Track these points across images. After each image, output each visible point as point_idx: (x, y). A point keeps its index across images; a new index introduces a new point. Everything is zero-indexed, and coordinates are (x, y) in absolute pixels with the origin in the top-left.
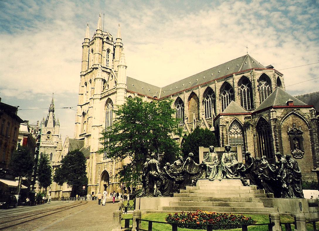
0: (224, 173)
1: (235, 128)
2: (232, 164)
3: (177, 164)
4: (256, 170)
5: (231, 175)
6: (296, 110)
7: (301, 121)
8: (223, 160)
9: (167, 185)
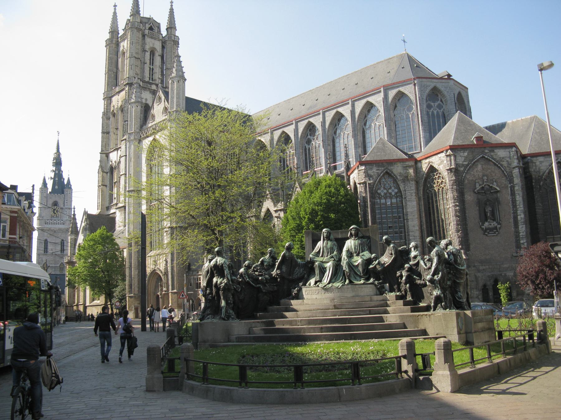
7: (497, 171)
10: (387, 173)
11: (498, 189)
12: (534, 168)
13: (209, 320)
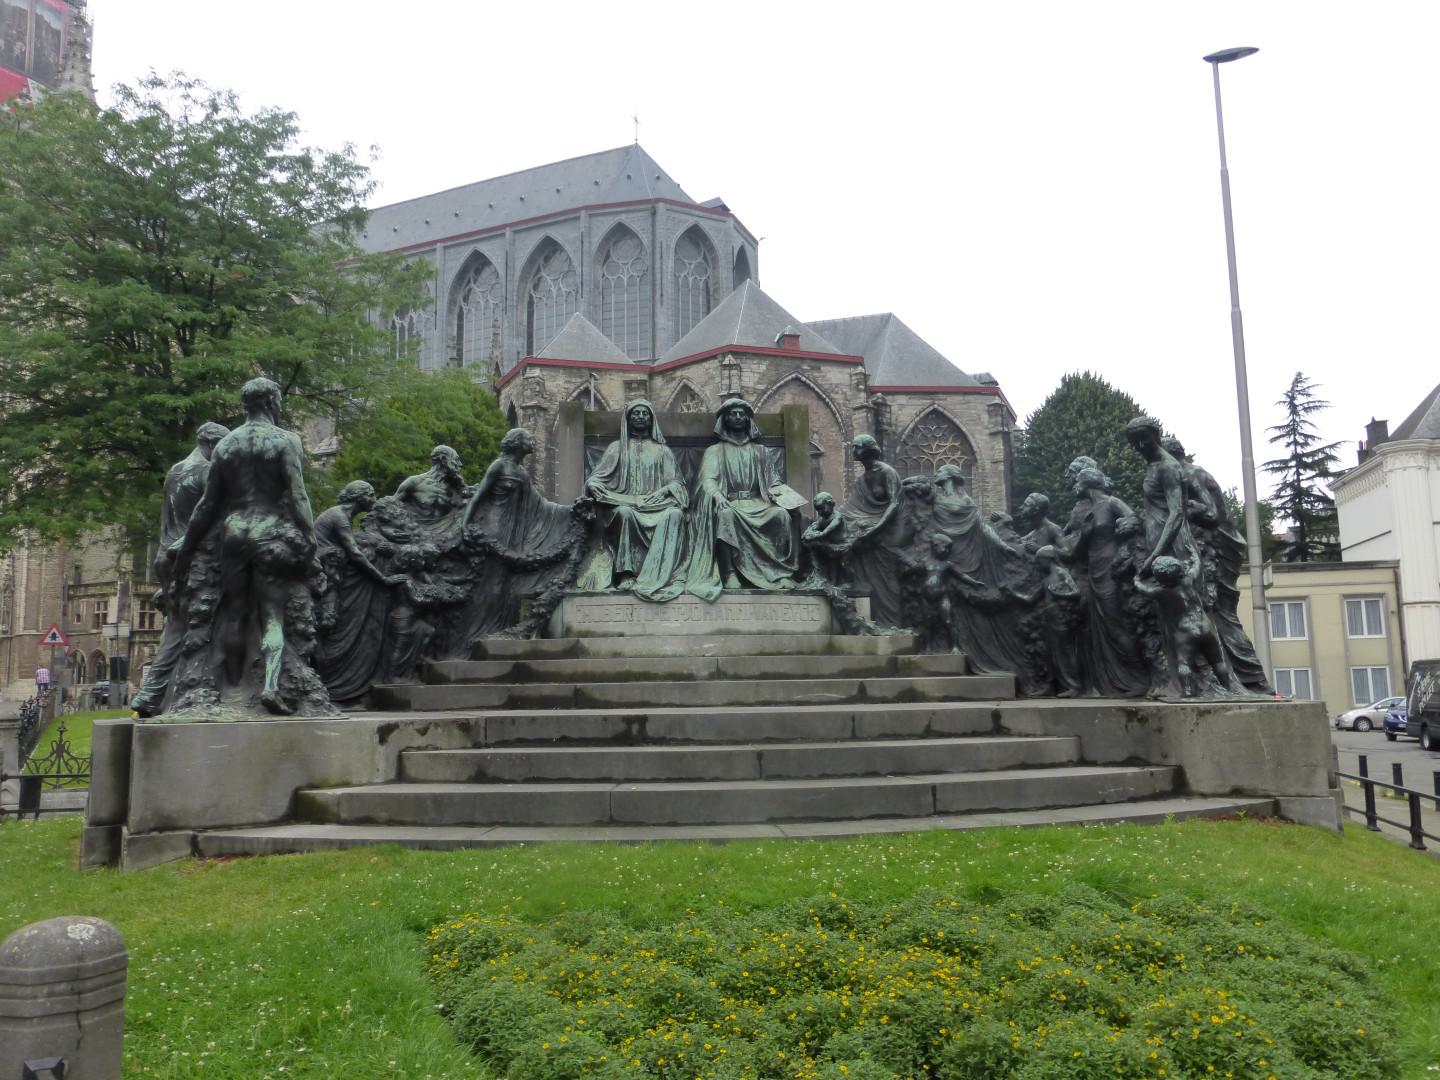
0: (725, 558)
2: (774, 503)
3: (425, 498)
4: (909, 541)
5: (771, 573)
6: (807, 371)
7: (822, 412)
8: (711, 487)
9: (352, 629)
11: (822, 450)
12: (888, 416)
13: (198, 713)
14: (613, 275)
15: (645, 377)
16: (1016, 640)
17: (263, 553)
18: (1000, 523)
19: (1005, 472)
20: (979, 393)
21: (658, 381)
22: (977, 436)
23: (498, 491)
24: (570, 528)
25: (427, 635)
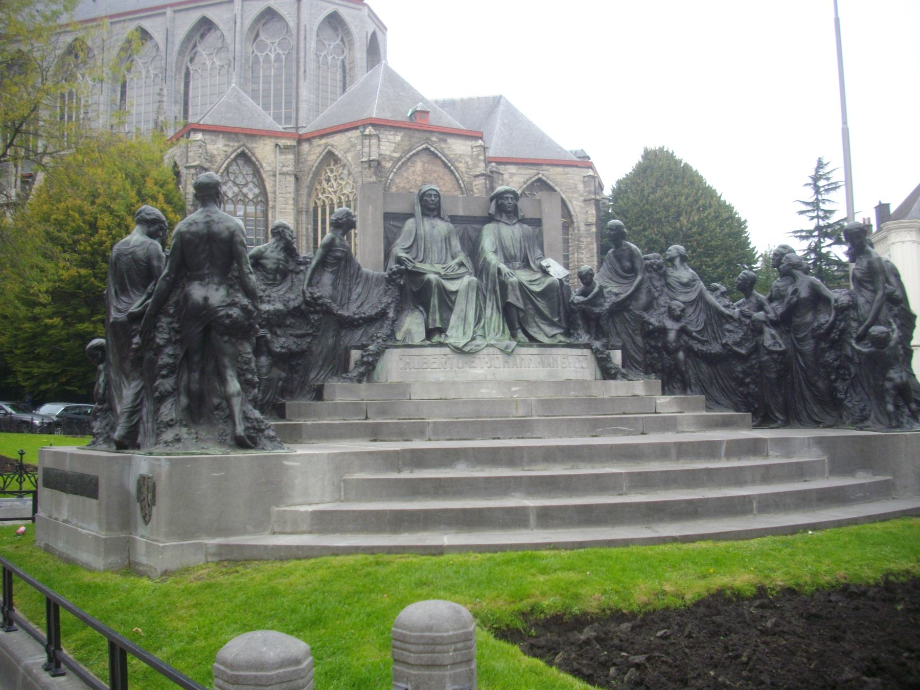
1: (240, 180)
3: (270, 264)
4: (648, 307)
6: (435, 142)
10: (243, 155)
14: (261, 52)
15: (294, 143)
16: (733, 384)
17: (222, 316)
18: (718, 293)
19: (597, 233)
20: (577, 166)
21: (305, 147)
22: (574, 202)
23: (330, 260)
24: (386, 292)
25: (280, 379)
